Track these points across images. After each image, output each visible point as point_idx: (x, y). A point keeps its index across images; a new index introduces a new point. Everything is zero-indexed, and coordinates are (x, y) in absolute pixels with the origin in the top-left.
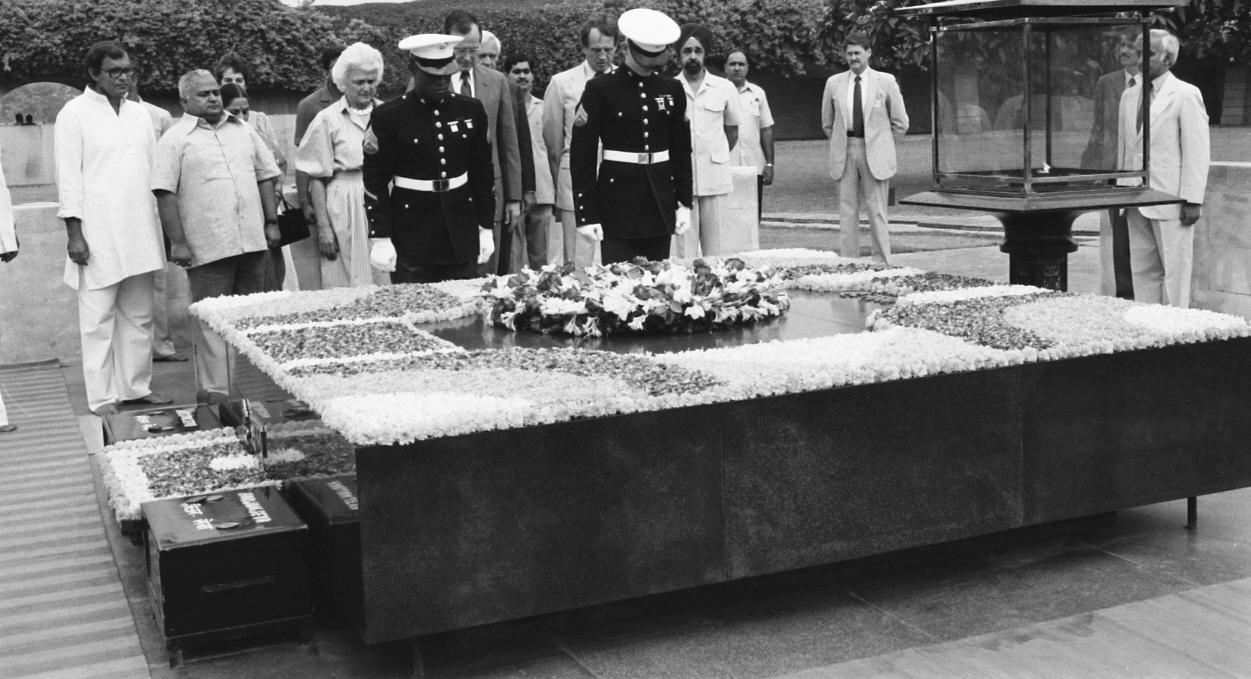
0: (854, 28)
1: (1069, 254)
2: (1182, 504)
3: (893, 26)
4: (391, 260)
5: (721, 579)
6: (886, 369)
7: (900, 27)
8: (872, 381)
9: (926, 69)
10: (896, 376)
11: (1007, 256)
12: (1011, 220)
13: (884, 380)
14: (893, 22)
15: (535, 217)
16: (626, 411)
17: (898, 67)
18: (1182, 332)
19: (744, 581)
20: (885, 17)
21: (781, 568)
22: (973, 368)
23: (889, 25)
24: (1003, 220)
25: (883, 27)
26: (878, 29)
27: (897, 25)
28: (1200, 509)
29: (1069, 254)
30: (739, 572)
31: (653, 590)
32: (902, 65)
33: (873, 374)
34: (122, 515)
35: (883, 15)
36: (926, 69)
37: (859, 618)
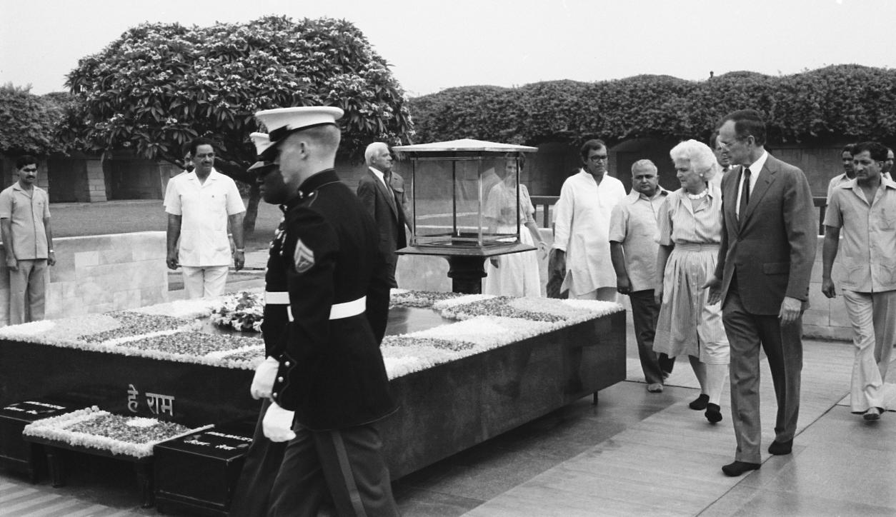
0: (92, 132)
1: (483, 279)
2: (593, 395)
3: (130, 132)
4: (49, 294)
5: (480, 441)
6: (525, 332)
7: (136, 133)
8: (521, 339)
9: (69, 155)
10: (529, 336)
11: (451, 279)
12: (454, 260)
13: (525, 338)
14: (129, 129)
15: (38, 267)
16: (453, 359)
17: (48, 154)
18: (602, 310)
19: (487, 441)
20: (123, 126)
21: (497, 434)
22: (536, 335)
23: (126, 131)
24: (448, 260)
25: (121, 133)
26: (118, 133)
27: (132, 131)
28: (599, 397)
29: (483, 279)
30: (486, 437)
31: (460, 449)
32: (50, 152)
33: (521, 336)
34: (148, 451)
35: (122, 124)
36: (69, 155)
37: (521, 456)
